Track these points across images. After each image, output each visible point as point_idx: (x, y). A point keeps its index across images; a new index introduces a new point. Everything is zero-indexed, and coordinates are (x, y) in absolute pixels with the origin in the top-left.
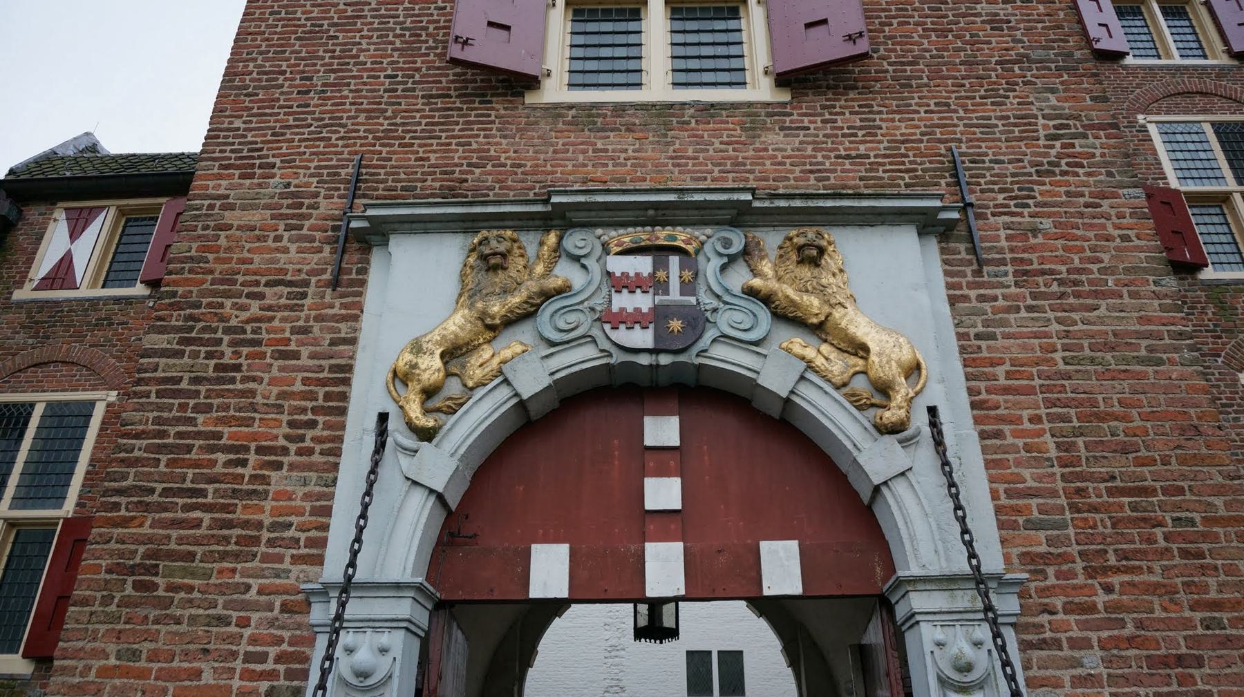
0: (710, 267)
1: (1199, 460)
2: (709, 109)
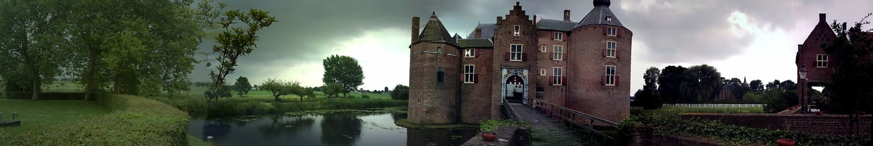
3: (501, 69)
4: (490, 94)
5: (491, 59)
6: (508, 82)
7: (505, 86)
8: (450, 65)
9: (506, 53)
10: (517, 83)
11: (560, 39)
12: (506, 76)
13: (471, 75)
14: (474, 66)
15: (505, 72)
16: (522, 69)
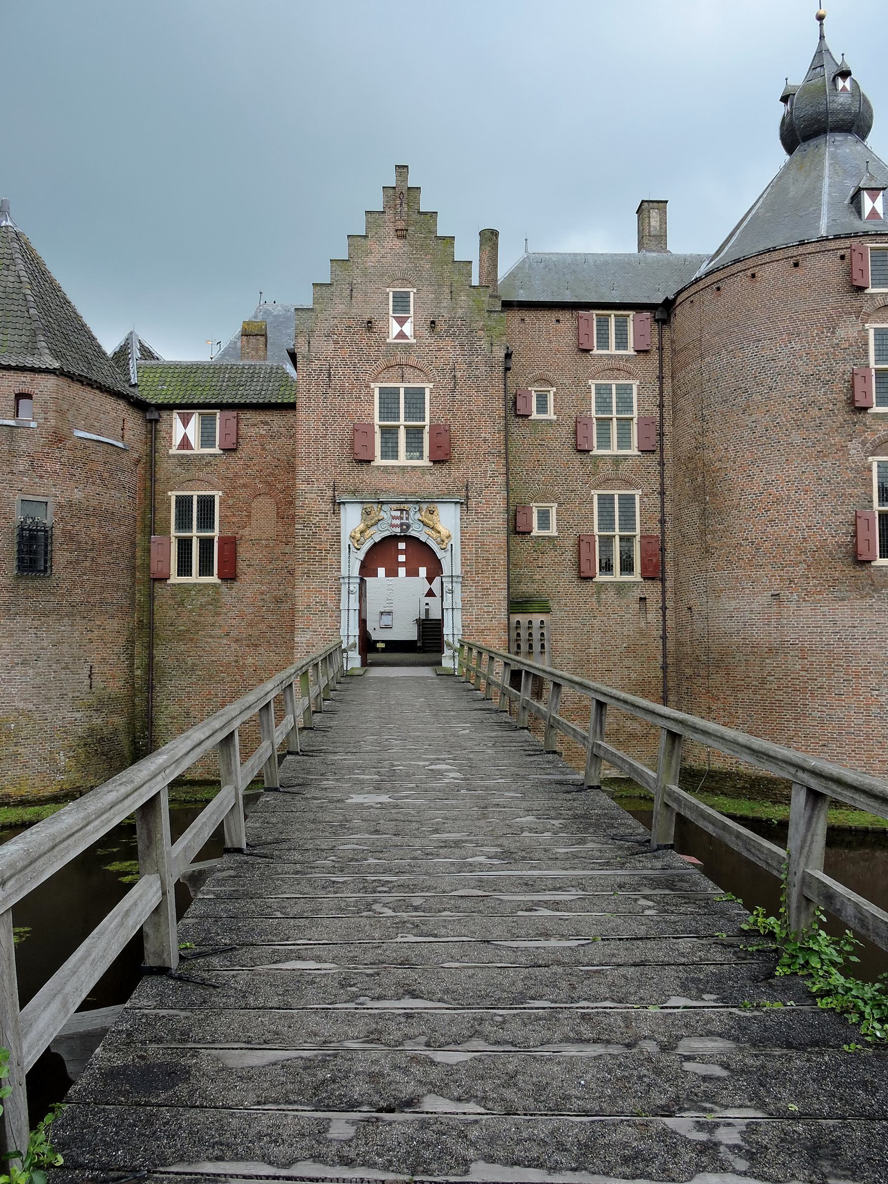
0: (411, 513)
1: (500, 554)
2: (414, 468)
3: (337, 505)
4: (292, 629)
6: (367, 569)
7: (355, 587)
8: (91, 489)
10: (412, 573)
11: (622, 343)
12: (357, 542)
13: (205, 544)
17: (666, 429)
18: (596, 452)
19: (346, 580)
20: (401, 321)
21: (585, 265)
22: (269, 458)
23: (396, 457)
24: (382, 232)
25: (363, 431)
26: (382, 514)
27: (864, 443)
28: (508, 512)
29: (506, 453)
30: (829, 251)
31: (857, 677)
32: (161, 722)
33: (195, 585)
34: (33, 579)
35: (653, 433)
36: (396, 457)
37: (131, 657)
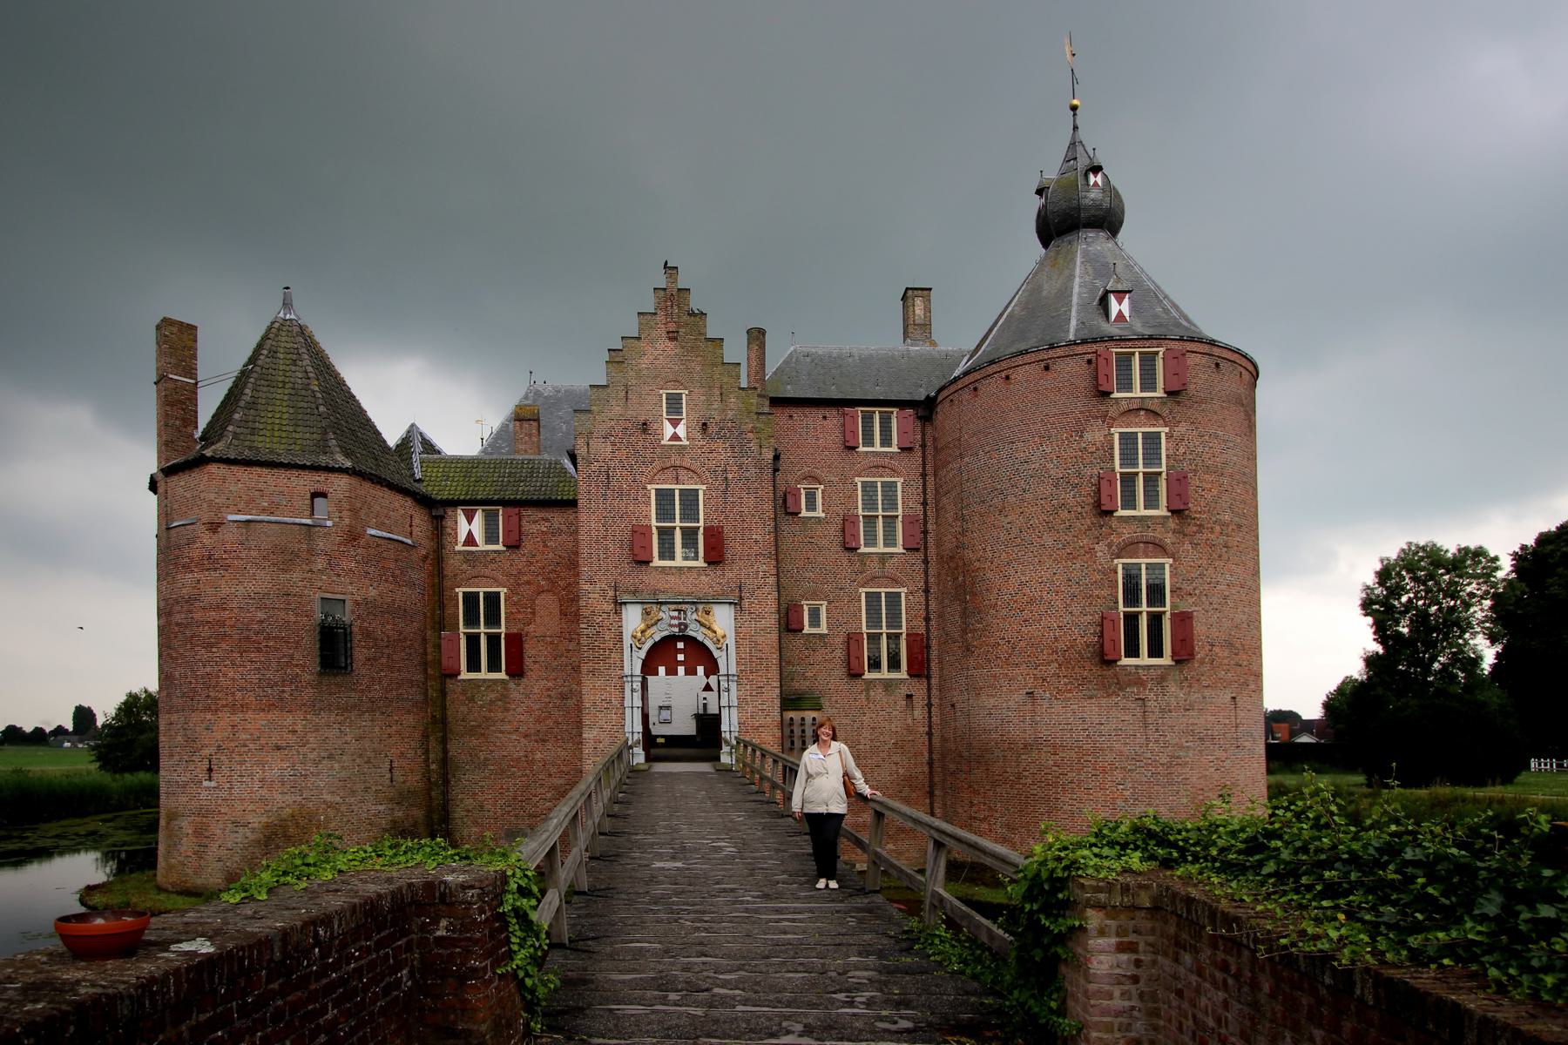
0: (689, 613)
3: (619, 605)
5: (572, 563)
6: (649, 668)
9: (634, 532)
10: (691, 671)
11: (886, 441)
12: (638, 640)
13: (493, 640)
14: (503, 591)
15: (632, 618)
16: (704, 603)
17: (930, 527)
18: (863, 550)
19: (629, 679)
20: (675, 423)
21: (850, 360)
22: (551, 555)
23: (673, 558)
24: (654, 334)
25: (641, 532)
26: (661, 614)
27: (1110, 546)
28: (779, 612)
29: (777, 554)
30: (1076, 355)
31: (1104, 772)
32: (457, 815)
33: (484, 680)
34: (335, 675)
35: (918, 529)
36: (673, 558)
37: (427, 752)
